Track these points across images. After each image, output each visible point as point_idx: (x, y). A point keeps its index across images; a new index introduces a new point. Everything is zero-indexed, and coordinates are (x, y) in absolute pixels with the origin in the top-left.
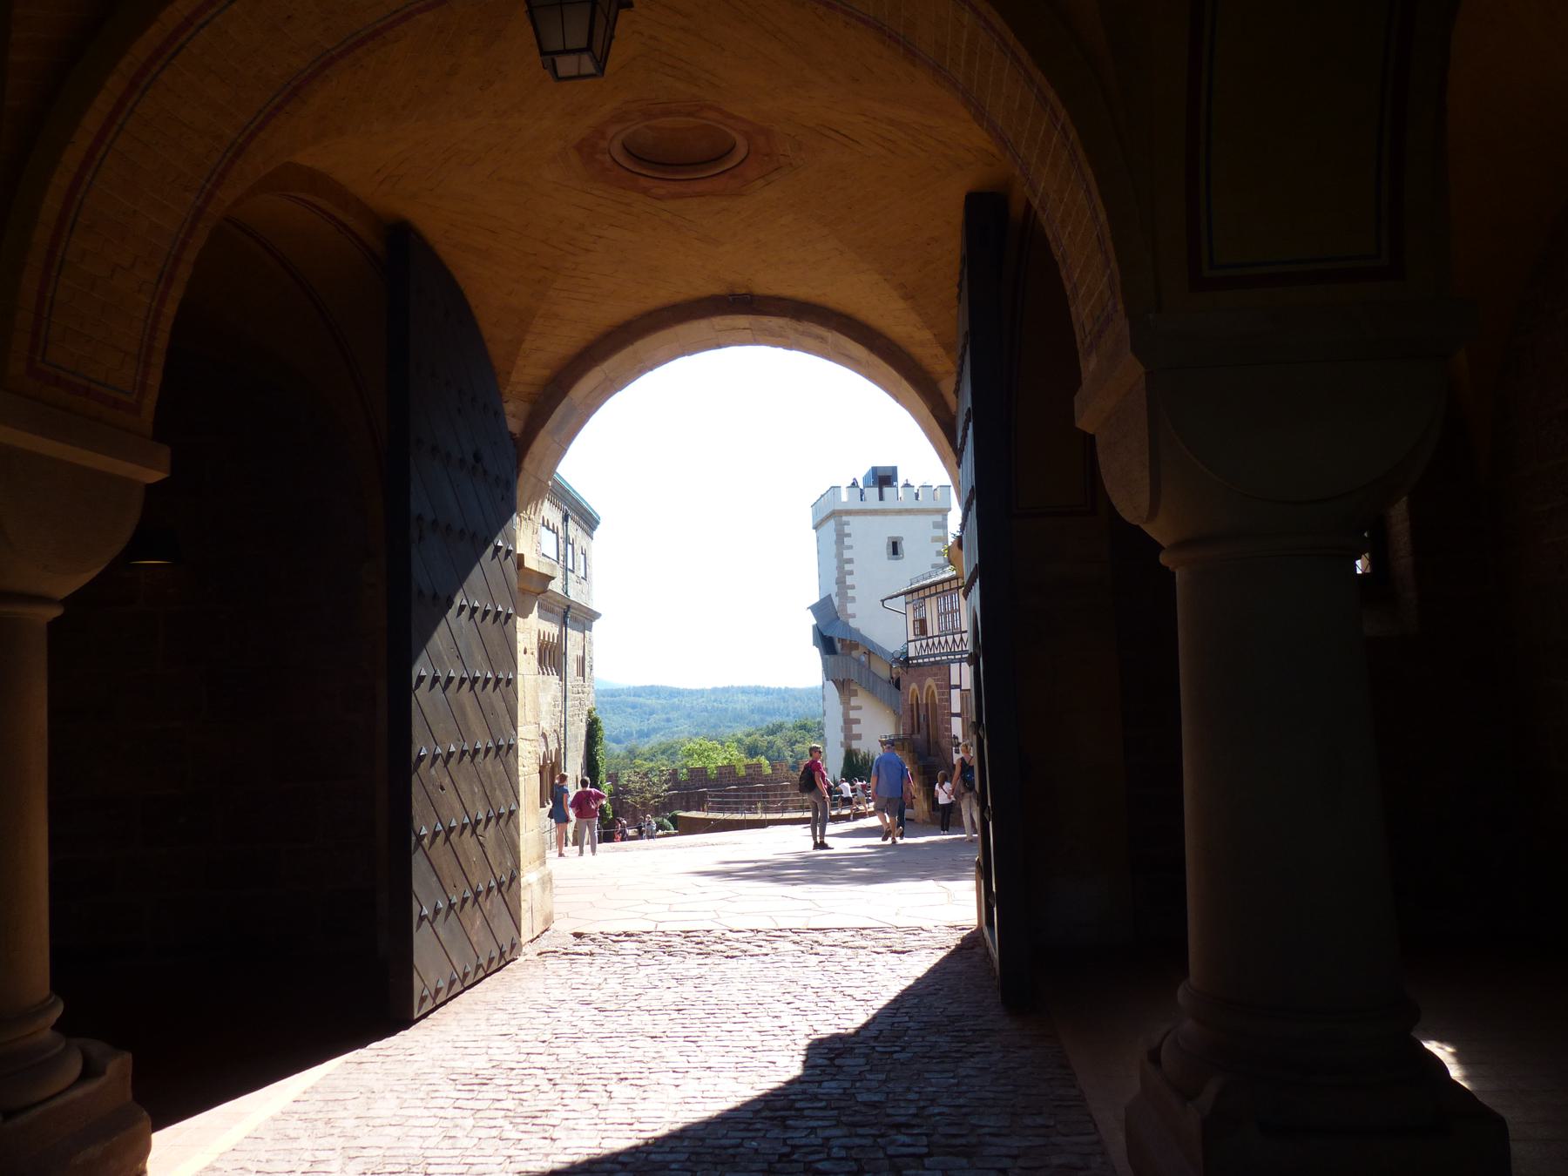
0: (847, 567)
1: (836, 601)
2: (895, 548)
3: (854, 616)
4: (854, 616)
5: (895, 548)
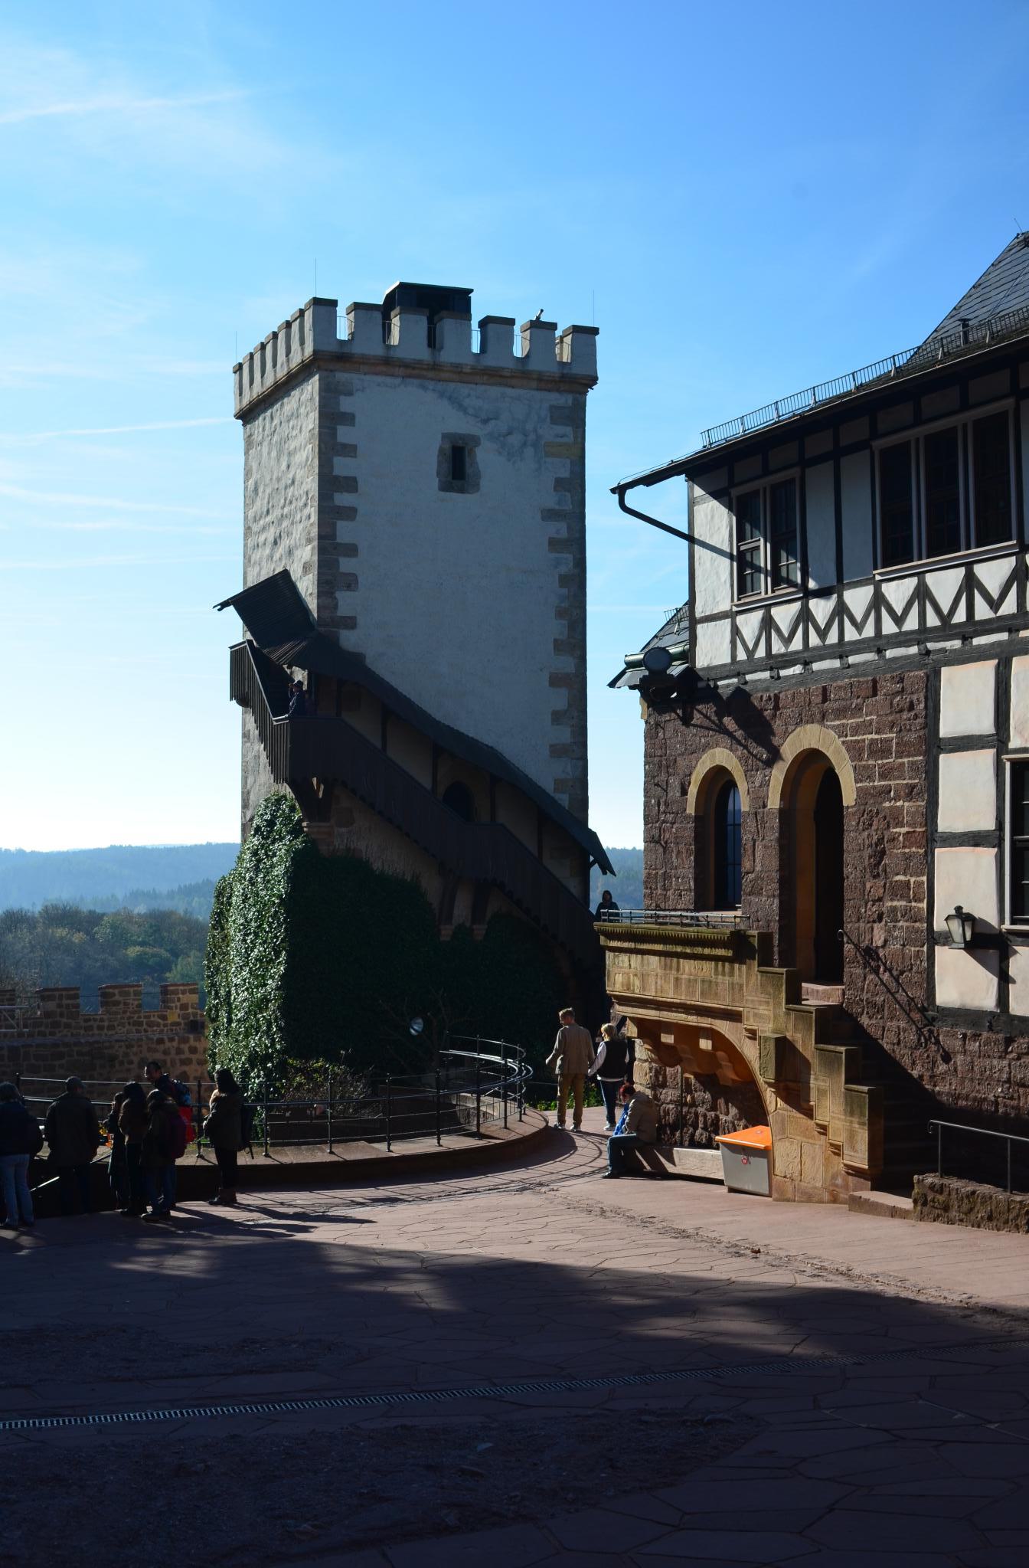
0: (343, 499)
1: (307, 586)
2: (457, 466)
3: (350, 623)
4: (350, 623)
5: (457, 466)
